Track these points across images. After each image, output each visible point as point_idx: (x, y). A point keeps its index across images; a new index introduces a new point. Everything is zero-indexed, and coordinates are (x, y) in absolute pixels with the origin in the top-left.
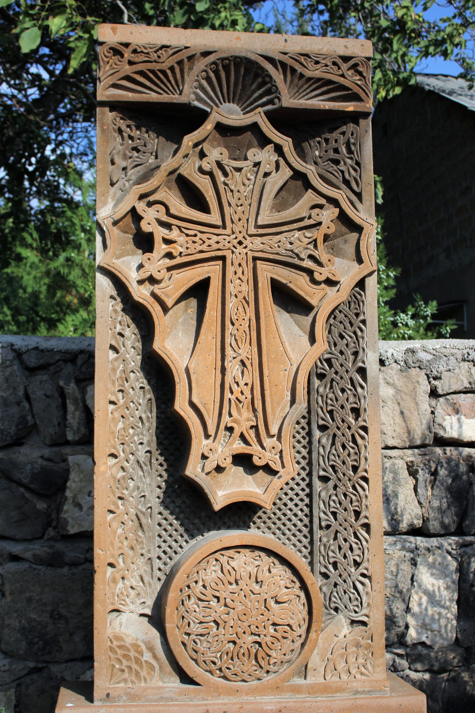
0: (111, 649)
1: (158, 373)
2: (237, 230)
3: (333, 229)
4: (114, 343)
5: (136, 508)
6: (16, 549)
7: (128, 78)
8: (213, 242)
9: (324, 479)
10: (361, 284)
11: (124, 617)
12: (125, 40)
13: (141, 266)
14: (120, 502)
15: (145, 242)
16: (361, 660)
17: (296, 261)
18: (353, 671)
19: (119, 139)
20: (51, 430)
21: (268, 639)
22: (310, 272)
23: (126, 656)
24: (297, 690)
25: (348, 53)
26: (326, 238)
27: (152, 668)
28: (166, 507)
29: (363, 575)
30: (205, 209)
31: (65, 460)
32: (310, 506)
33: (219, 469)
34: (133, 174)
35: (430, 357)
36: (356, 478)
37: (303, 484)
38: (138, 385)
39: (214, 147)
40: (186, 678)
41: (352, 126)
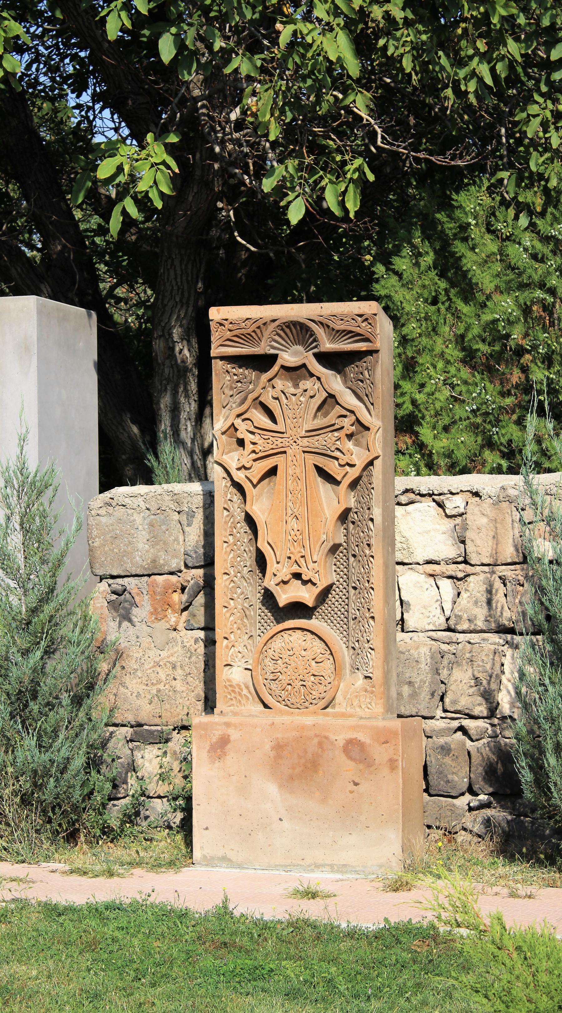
0: (226, 687)
4: (226, 506)
5: (242, 605)
8: (278, 442)
10: (371, 463)
11: (234, 669)
14: (232, 602)
18: (363, 707)
21: (310, 683)
23: (233, 691)
24: (327, 715)
25: (361, 312)
27: (248, 698)
28: (263, 605)
33: (285, 583)
34: (238, 398)
38: (242, 531)
40: (266, 706)
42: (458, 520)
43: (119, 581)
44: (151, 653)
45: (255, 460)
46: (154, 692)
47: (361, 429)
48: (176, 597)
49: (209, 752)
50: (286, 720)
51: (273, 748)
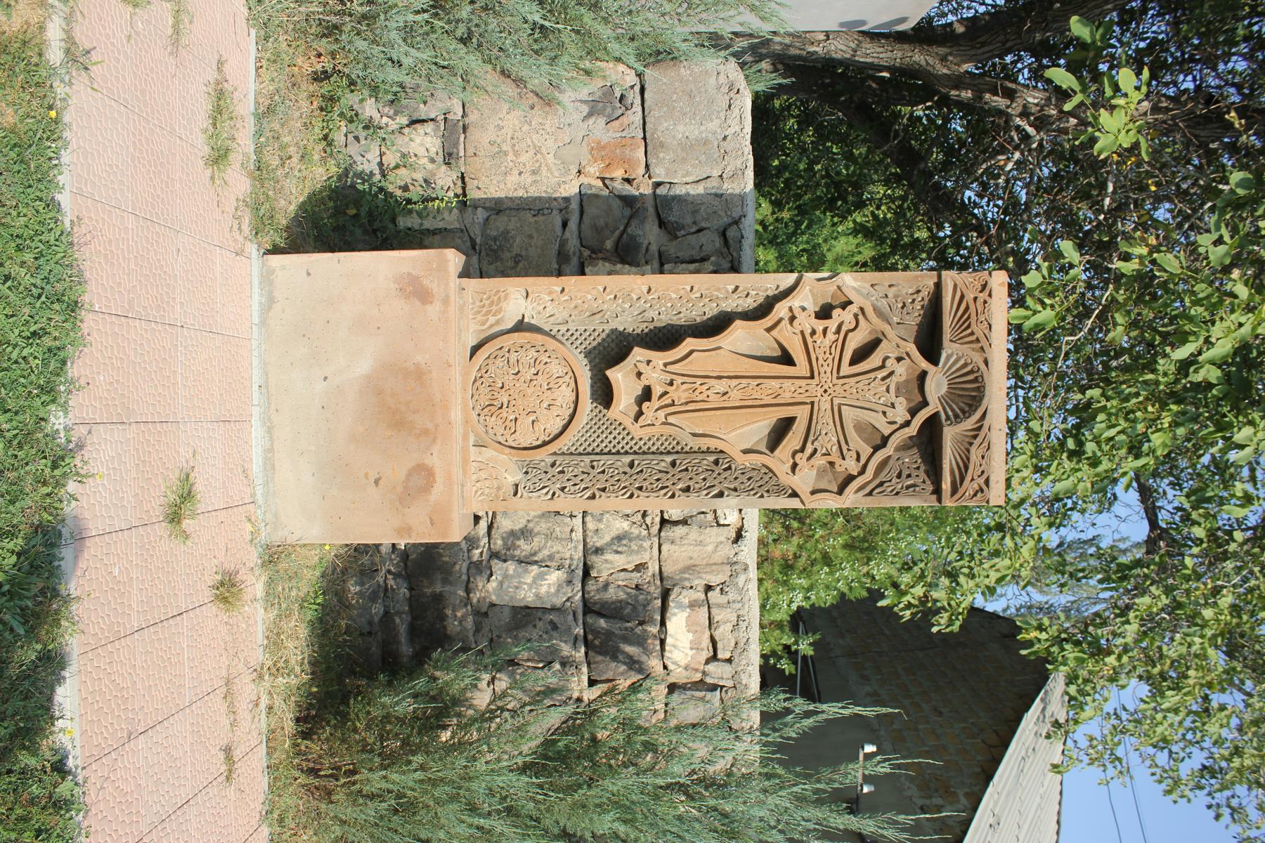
1: (716, 326)
2: (836, 388)
3: (838, 469)
6: (573, 225)
7: (962, 297)
9: (631, 465)
10: (794, 494)
12: (993, 293)
13: (804, 309)
15: (824, 313)
16: (487, 491)
17: (811, 438)
19: (911, 291)
20: (672, 251)
21: (505, 415)
22: (802, 450)
23: (492, 304)
25: (992, 483)
26: (832, 464)
27: (483, 324)
28: (608, 336)
29: (554, 494)
30: (852, 363)
31: (647, 263)
32: (609, 453)
33: (639, 374)
35: (741, 584)
36: (632, 489)
37: (627, 448)
38: (707, 310)
39: (907, 370)
40: (475, 349)
41: (931, 488)
42: (710, 517)
43: (638, 101)
44: (550, 143)
45: (802, 332)
46: (505, 148)
47: (840, 480)
48: (619, 174)
49: (409, 274)
50: (455, 381)
51: (417, 365)
